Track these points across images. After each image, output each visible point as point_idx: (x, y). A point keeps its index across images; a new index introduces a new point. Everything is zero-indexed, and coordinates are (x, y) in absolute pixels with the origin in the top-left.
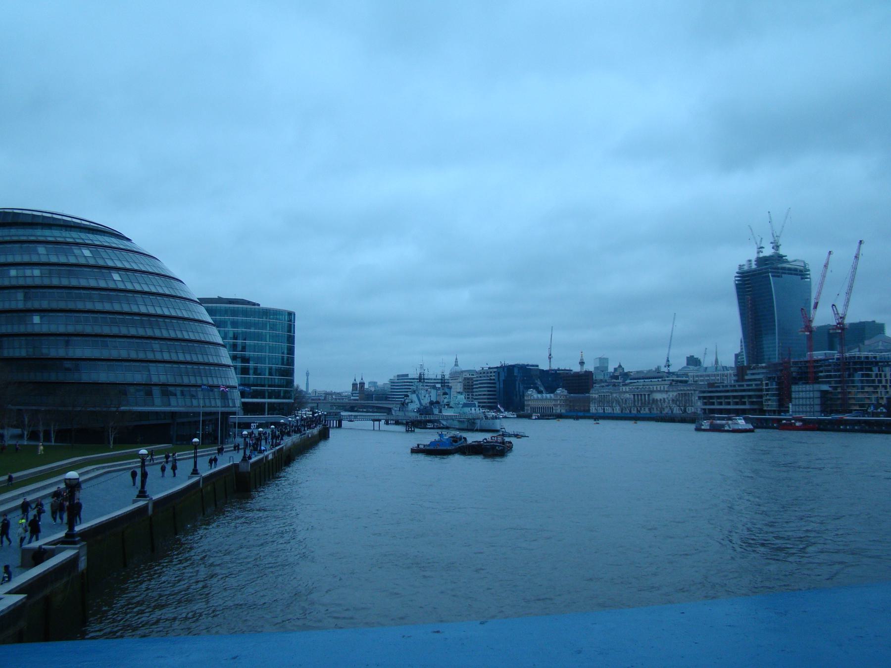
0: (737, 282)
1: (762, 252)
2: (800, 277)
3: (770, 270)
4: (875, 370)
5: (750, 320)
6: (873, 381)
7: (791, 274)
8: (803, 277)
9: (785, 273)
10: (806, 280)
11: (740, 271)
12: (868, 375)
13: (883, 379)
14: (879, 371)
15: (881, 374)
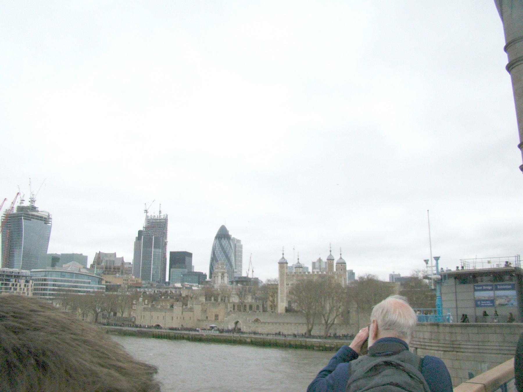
0: (2, 220)
1: (23, 203)
2: (44, 222)
3: (23, 215)
4: (13, 280)
5: (7, 246)
6: (11, 288)
7: (38, 219)
8: (46, 222)
9: (34, 218)
10: (49, 224)
11: (6, 213)
12: (6, 284)
13: (18, 287)
14: (16, 282)
15: (16, 285)
